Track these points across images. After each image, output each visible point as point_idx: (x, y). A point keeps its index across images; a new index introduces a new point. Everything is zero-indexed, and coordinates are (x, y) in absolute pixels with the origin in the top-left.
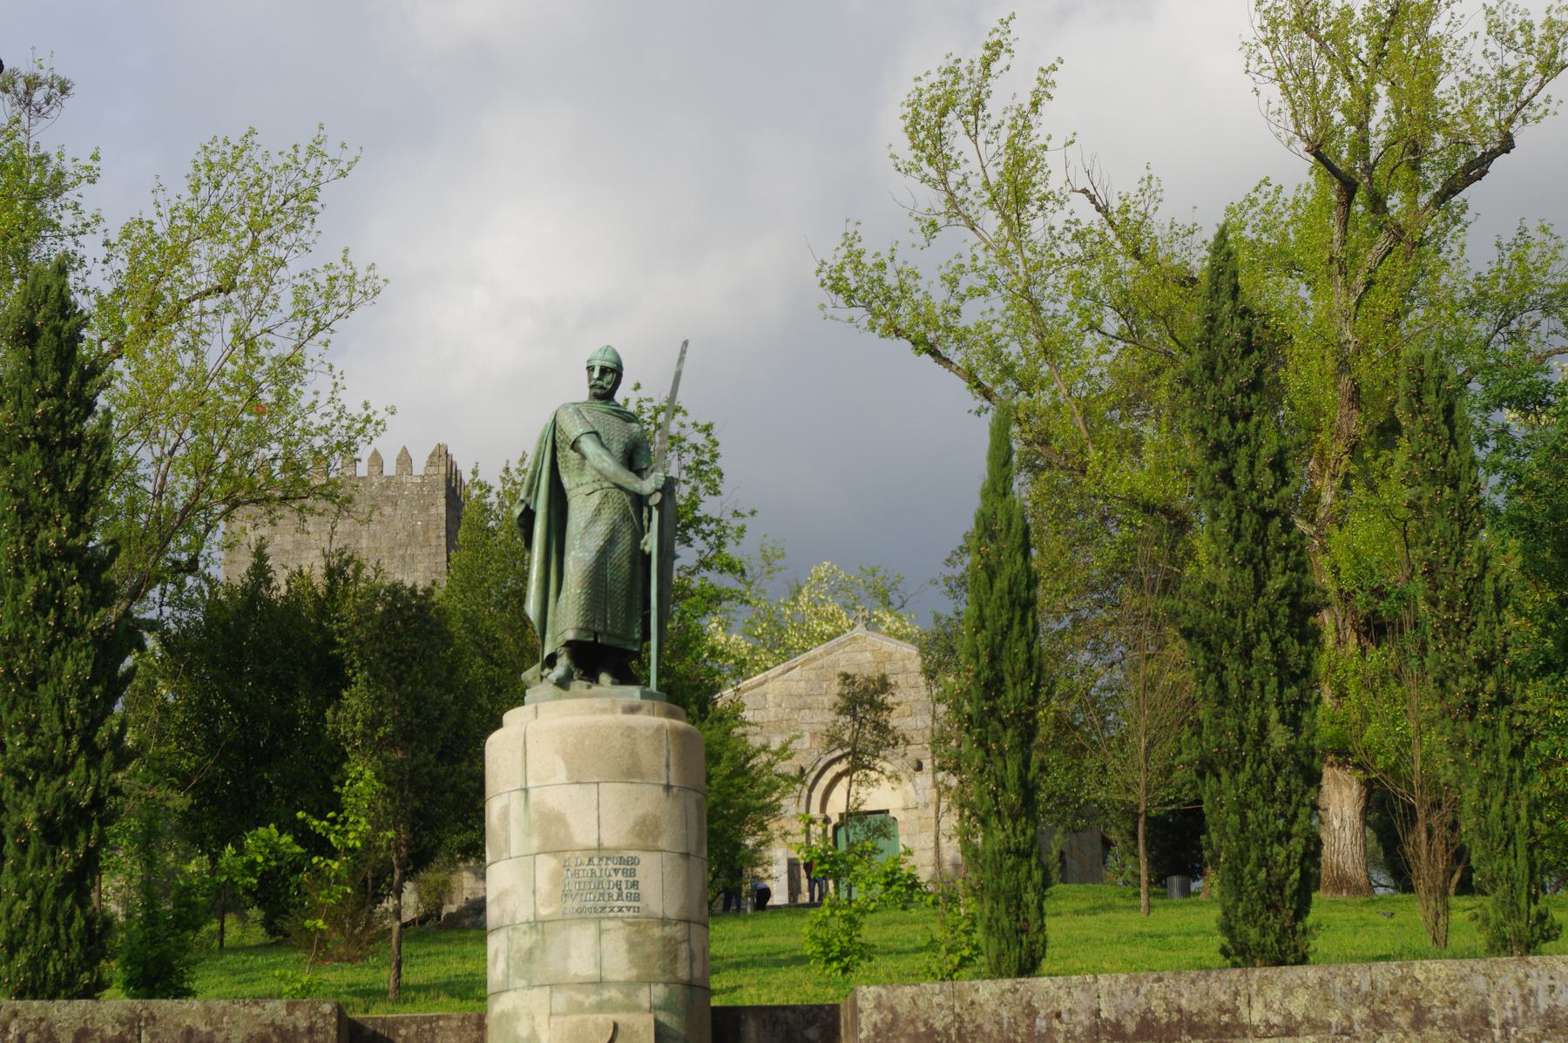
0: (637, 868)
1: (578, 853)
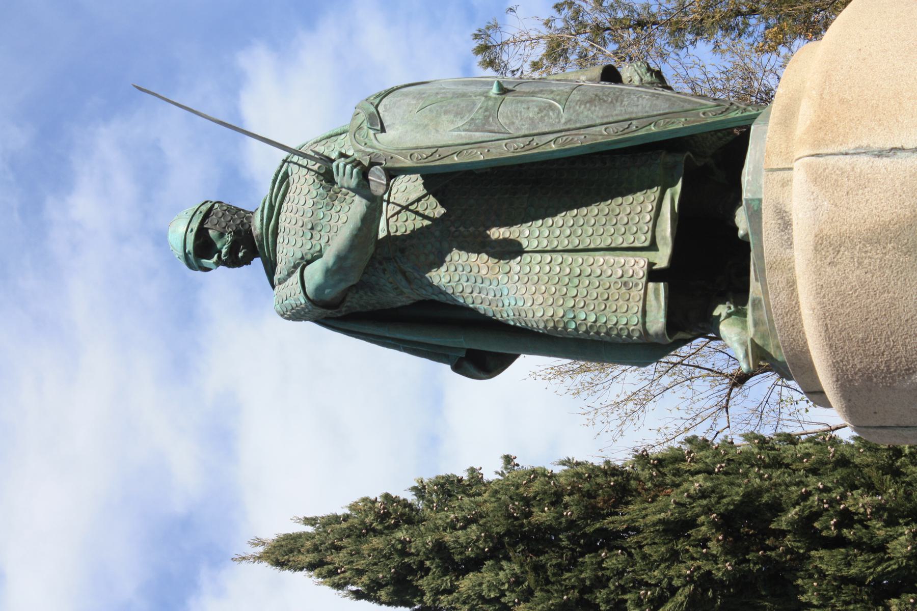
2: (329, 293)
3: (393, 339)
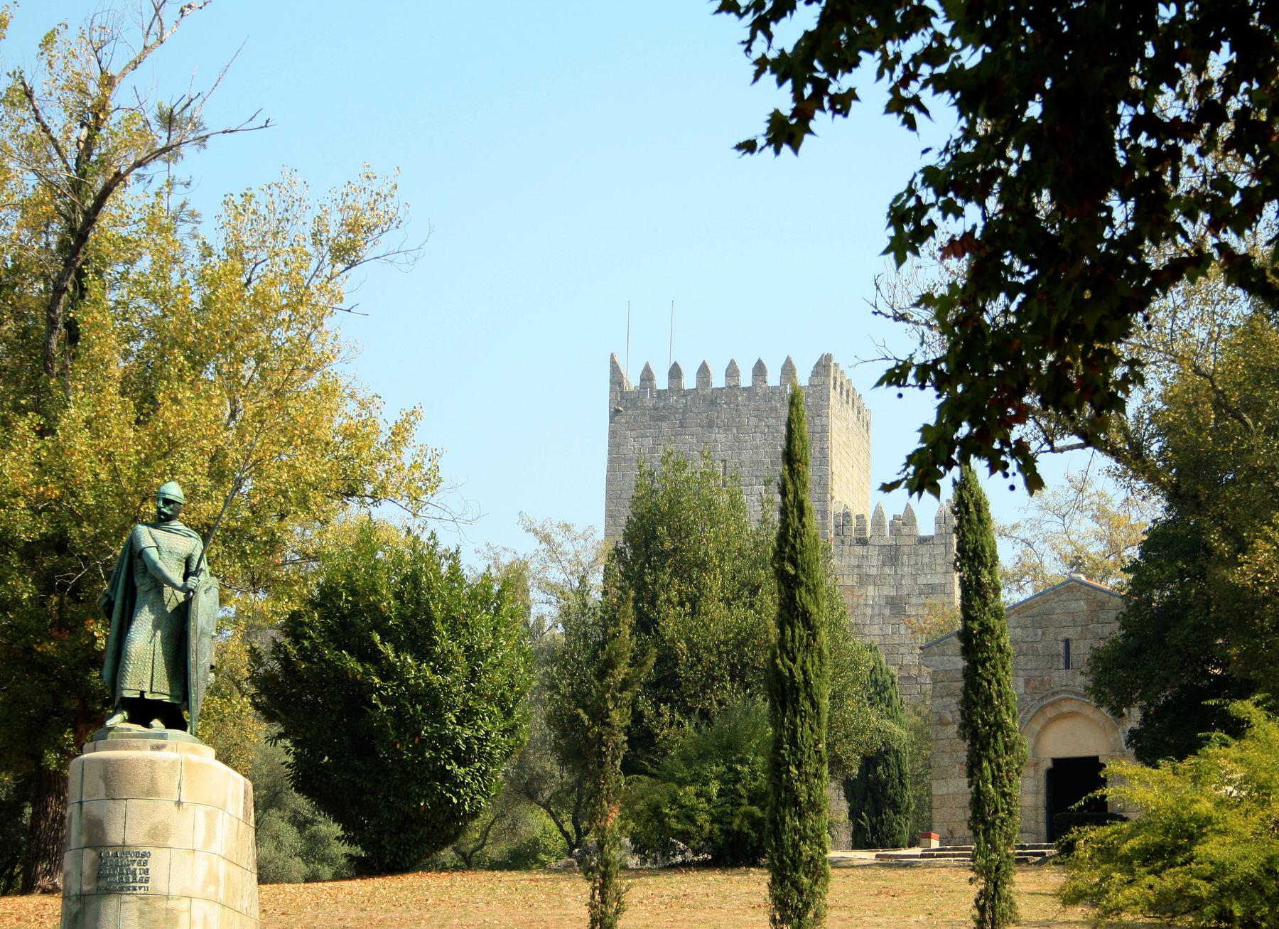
0: (150, 861)
2: (144, 556)
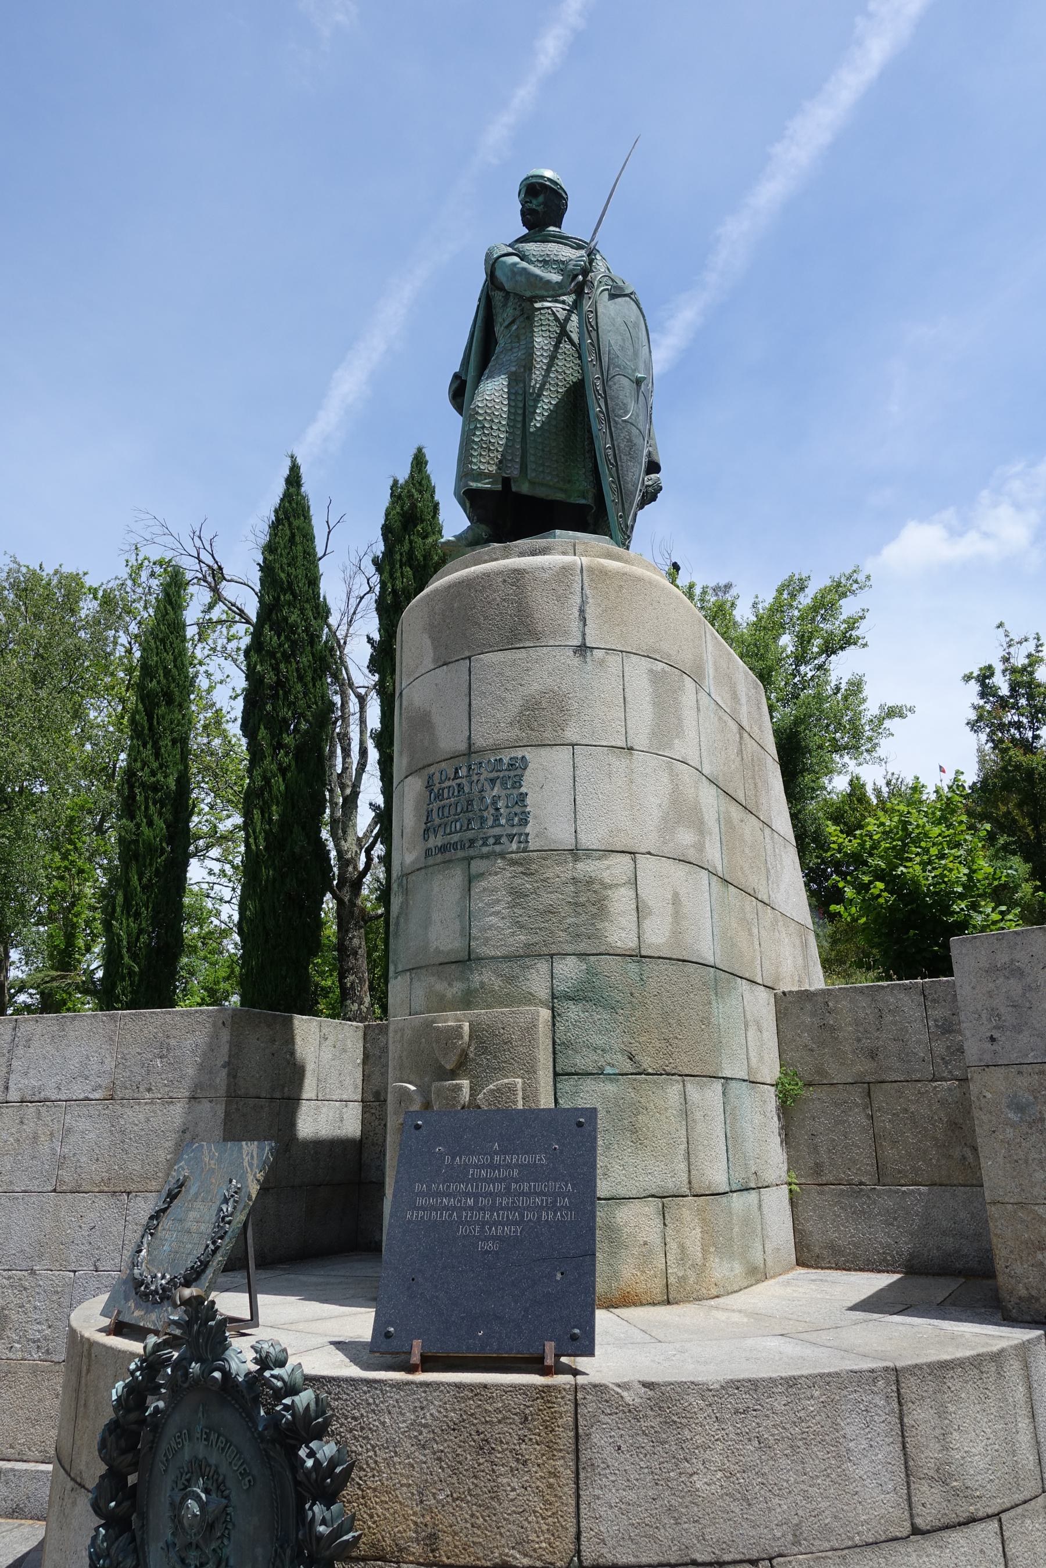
1: (443, 764)
3: (474, 331)
